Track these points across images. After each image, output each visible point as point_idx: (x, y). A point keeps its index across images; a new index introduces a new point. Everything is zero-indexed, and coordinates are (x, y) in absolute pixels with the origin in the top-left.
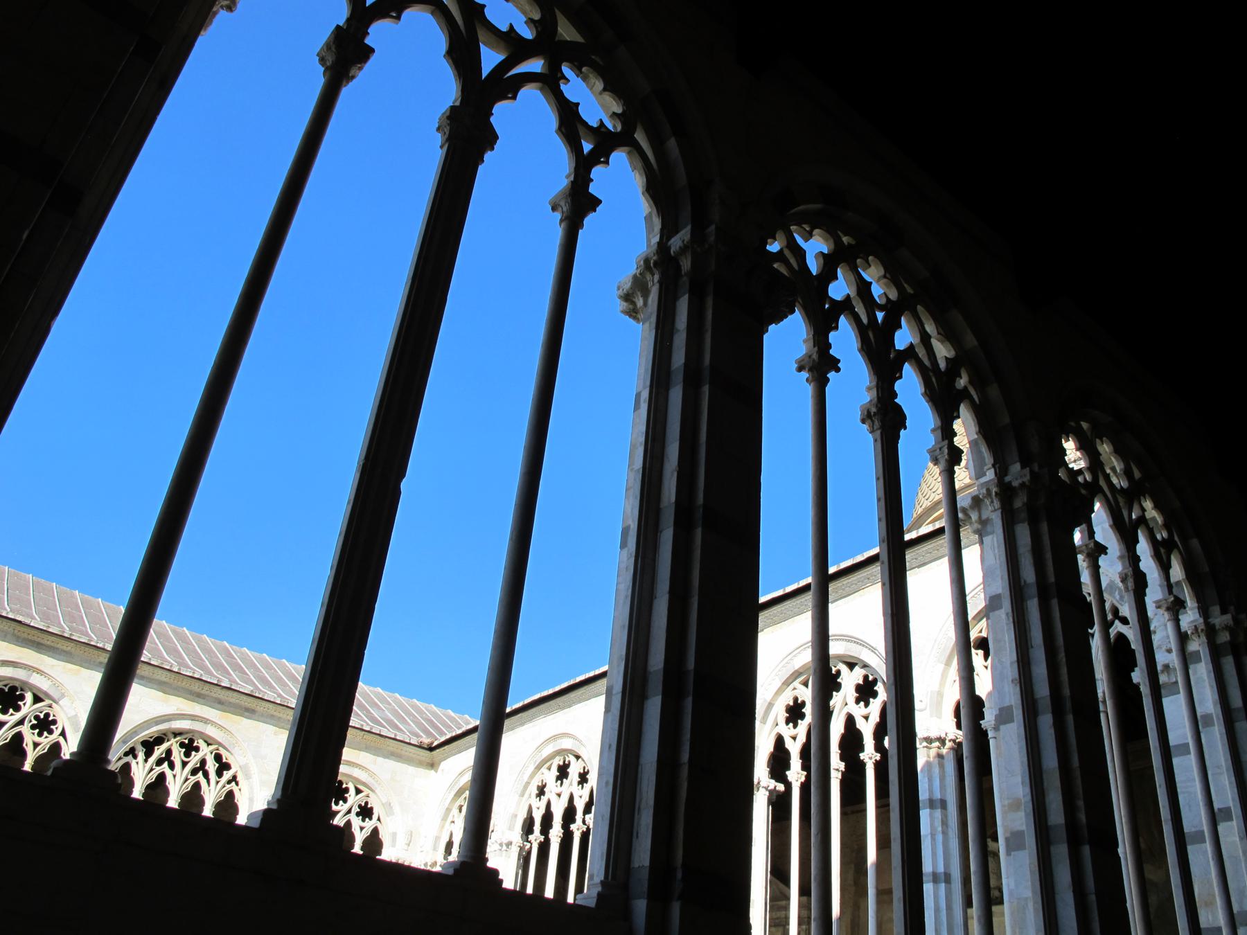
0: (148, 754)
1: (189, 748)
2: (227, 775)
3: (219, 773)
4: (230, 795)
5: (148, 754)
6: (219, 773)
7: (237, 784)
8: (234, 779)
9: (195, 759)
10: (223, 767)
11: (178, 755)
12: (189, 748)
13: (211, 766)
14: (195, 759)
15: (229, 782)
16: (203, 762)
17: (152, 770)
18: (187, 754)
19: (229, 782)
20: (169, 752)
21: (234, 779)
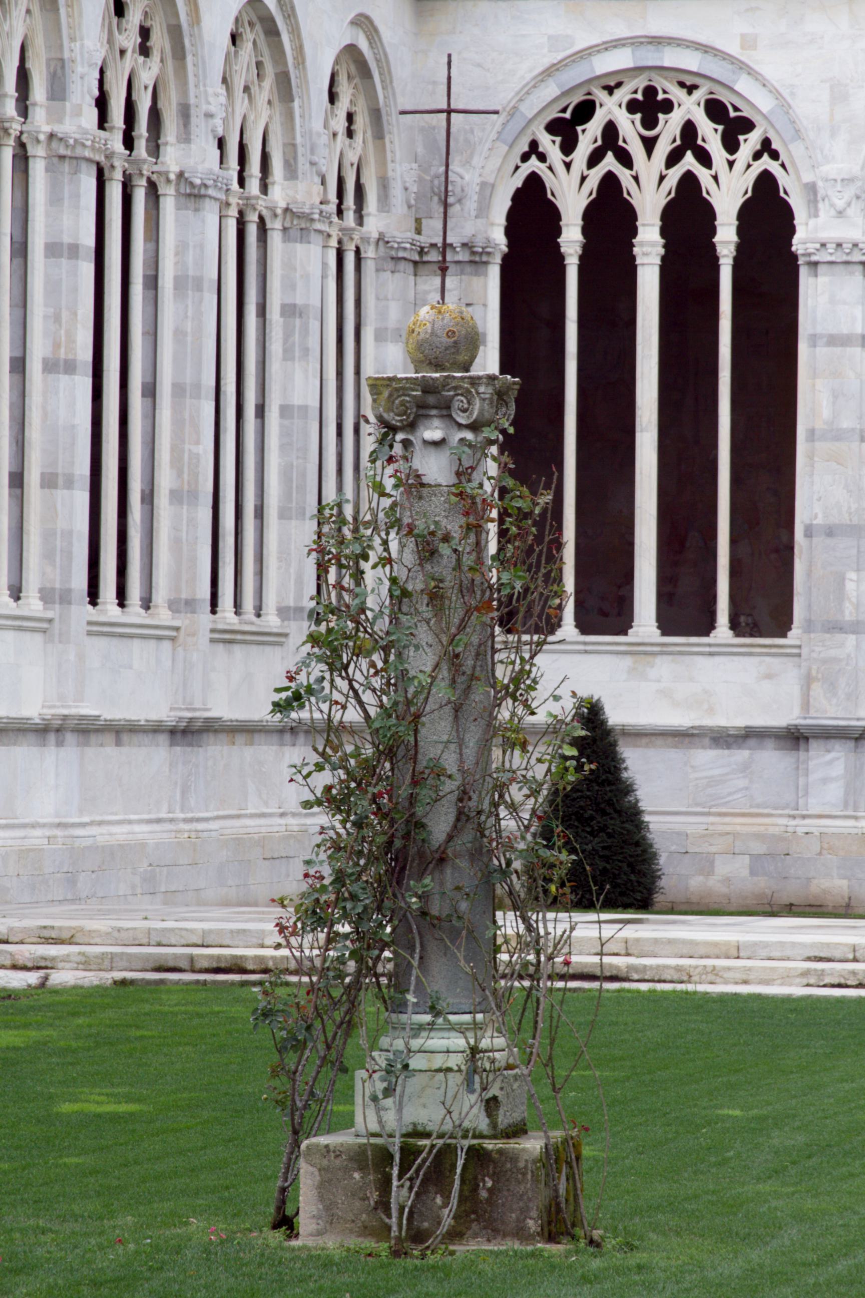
0: (568, 147)
1: (650, 107)
2: (750, 143)
3: (731, 145)
4: (766, 182)
5: (568, 147)
6: (731, 145)
7: (775, 155)
8: (766, 148)
9: (669, 128)
10: (734, 128)
11: (630, 128)
12: (650, 107)
13: (710, 134)
14: (669, 128)
15: (757, 156)
16: (689, 130)
17: (583, 179)
18: (650, 122)
19: (757, 156)
20: (610, 130)
21: (766, 148)
